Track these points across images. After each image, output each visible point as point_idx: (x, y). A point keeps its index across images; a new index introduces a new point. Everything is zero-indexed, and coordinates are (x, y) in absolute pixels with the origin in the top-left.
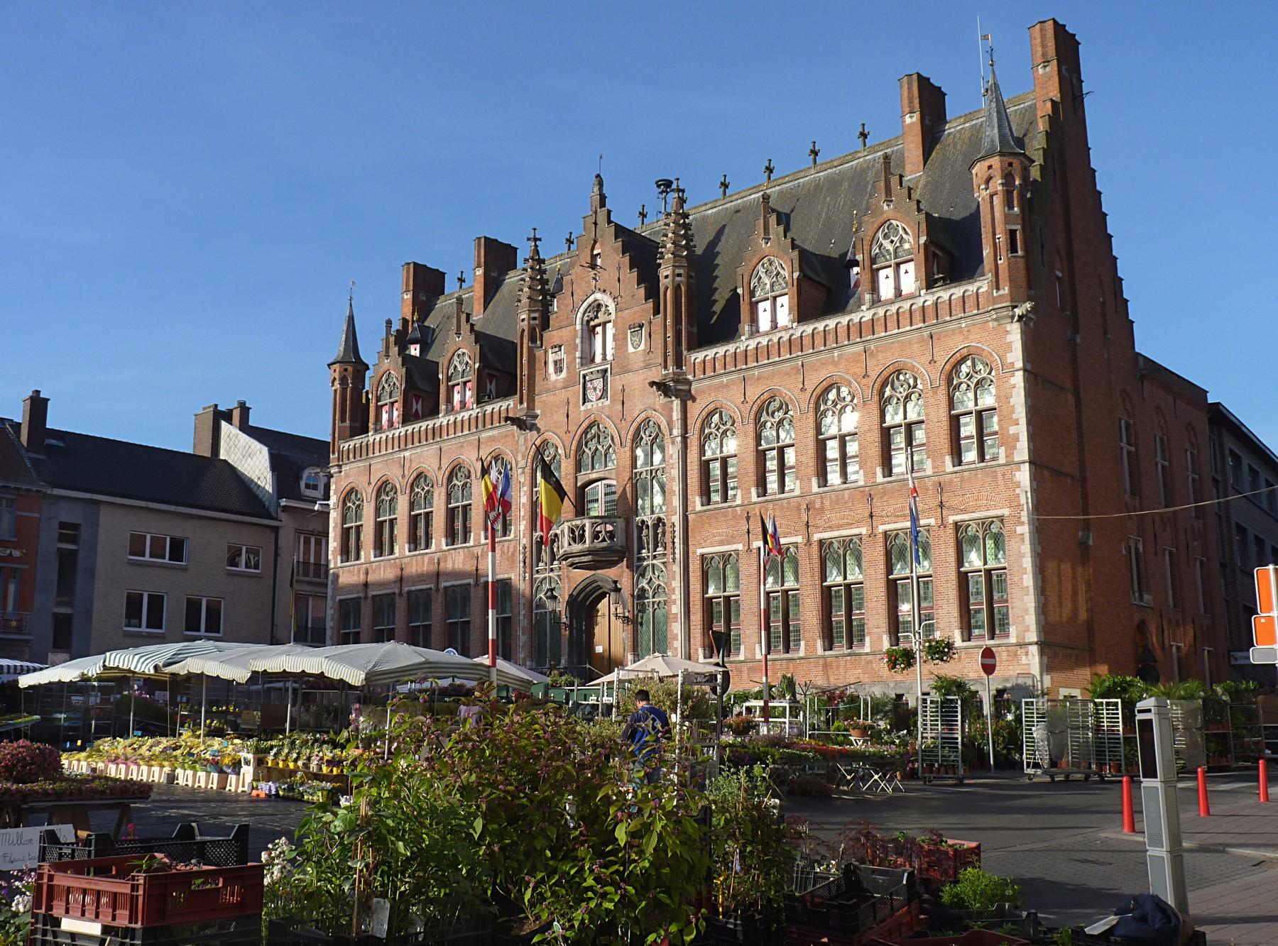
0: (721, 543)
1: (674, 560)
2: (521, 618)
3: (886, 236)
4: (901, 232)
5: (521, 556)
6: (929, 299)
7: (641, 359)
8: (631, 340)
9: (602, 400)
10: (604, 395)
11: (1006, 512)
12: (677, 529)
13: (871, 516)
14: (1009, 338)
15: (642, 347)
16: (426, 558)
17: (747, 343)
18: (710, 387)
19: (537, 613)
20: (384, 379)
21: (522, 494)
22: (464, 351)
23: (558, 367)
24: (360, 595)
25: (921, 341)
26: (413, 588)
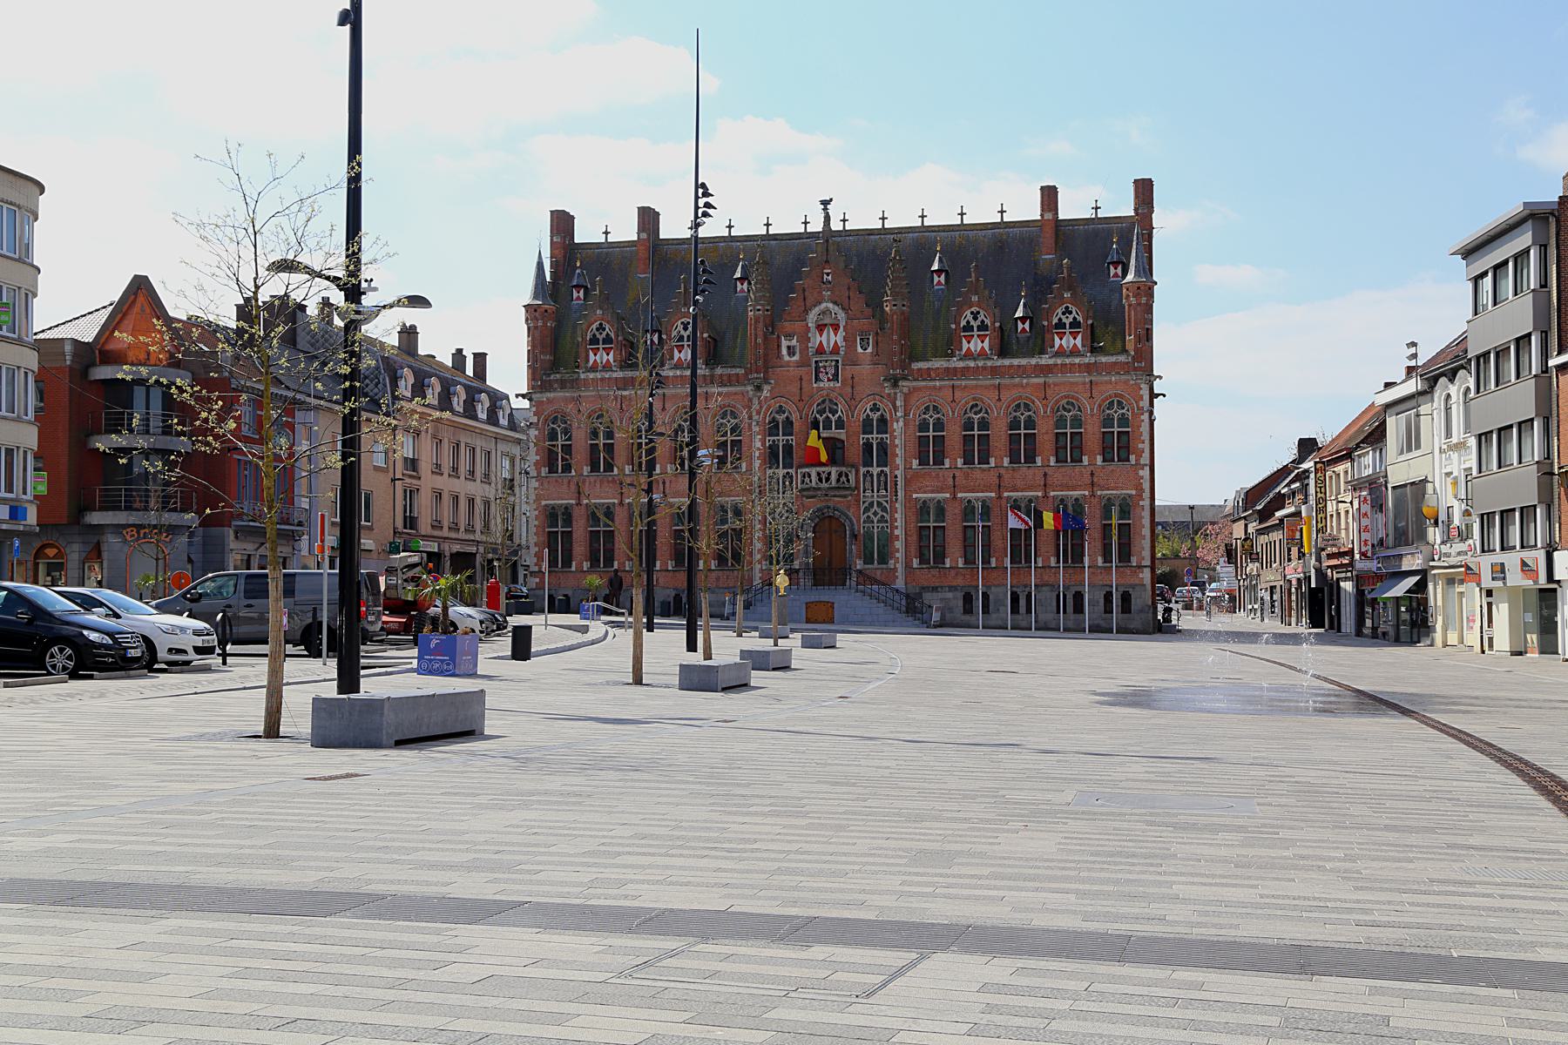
0: (932, 492)
1: (896, 500)
3: (1064, 313)
4: (1074, 312)
7: (869, 358)
10: (836, 375)
11: (1134, 492)
12: (899, 479)
13: (1045, 485)
14: (1141, 392)
15: (870, 350)
24: (571, 501)
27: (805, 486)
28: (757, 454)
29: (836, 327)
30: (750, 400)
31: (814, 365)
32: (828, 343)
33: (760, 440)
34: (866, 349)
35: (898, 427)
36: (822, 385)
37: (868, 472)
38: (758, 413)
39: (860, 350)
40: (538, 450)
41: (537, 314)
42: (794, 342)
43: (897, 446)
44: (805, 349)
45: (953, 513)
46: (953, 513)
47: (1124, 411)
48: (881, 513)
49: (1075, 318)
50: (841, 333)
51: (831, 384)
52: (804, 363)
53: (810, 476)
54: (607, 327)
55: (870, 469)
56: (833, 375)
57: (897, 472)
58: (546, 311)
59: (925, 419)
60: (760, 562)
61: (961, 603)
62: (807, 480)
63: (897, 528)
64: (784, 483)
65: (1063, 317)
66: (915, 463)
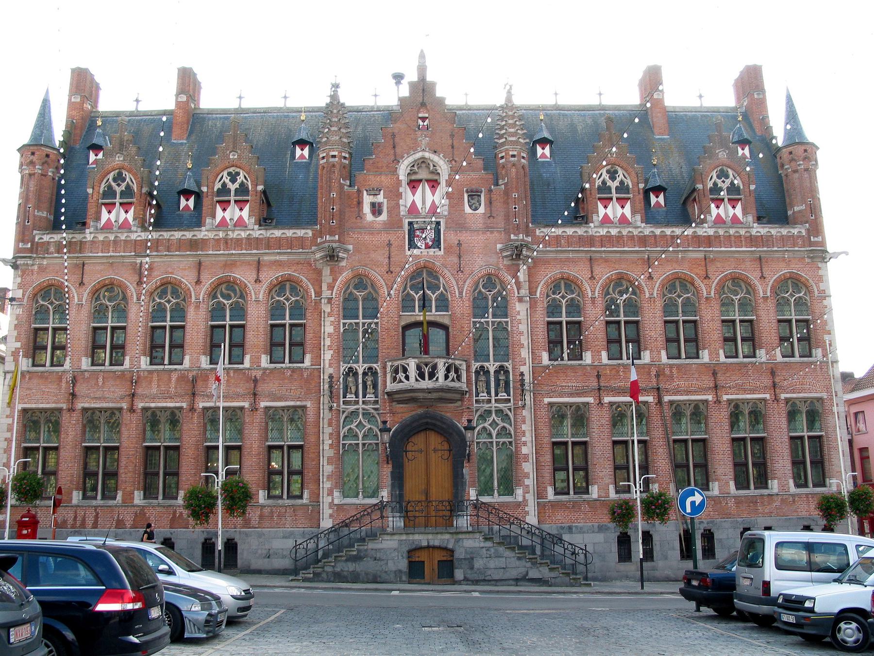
0: (571, 395)
2: (326, 447)
5: (327, 386)
6: (759, 230)
7: (481, 221)
8: (469, 201)
9: (432, 250)
10: (437, 243)
15: (481, 210)
16: (174, 377)
17: (596, 230)
18: (556, 259)
19: (344, 445)
20: (111, 176)
21: (327, 323)
22: (238, 170)
23: (376, 209)
25: (754, 260)
26: (153, 405)
27: (397, 387)
28: (328, 342)
29: (434, 184)
30: (319, 273)
31: (406, 227)
32: (424, 203)
33: (332, 323)
34: (476, 209)
35: (520, 310)
36: (416, 252)
37: (482, 367)
38: (331, 287)
39: (468, 210)
40: (19, 334)
41: (35, 158)
42: (380, 198)
43: (521, 333)
44: (394, 209)
45: (599, 422)
46: (599, 422)
47: (801, 295)
48: (502, 424)
49: (732, 183)
50: (443, 188)
51: (431, 251)
52: (394, 223)
53: (405, 370)
54: (128, 176)
55: (486, 364)
56: (433, 241)
57: (523, 369)
58: (47, 156)
59: (554, 299)
60: (330, 493)
61: (615, 547)
62: (401, 375)
63: (525, 444)
64: (364, 383)
65: (719, 182)
66: (545, 356)
